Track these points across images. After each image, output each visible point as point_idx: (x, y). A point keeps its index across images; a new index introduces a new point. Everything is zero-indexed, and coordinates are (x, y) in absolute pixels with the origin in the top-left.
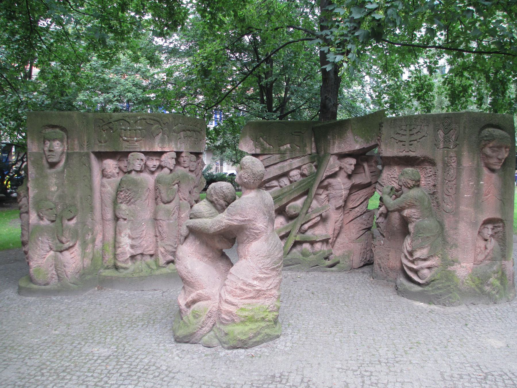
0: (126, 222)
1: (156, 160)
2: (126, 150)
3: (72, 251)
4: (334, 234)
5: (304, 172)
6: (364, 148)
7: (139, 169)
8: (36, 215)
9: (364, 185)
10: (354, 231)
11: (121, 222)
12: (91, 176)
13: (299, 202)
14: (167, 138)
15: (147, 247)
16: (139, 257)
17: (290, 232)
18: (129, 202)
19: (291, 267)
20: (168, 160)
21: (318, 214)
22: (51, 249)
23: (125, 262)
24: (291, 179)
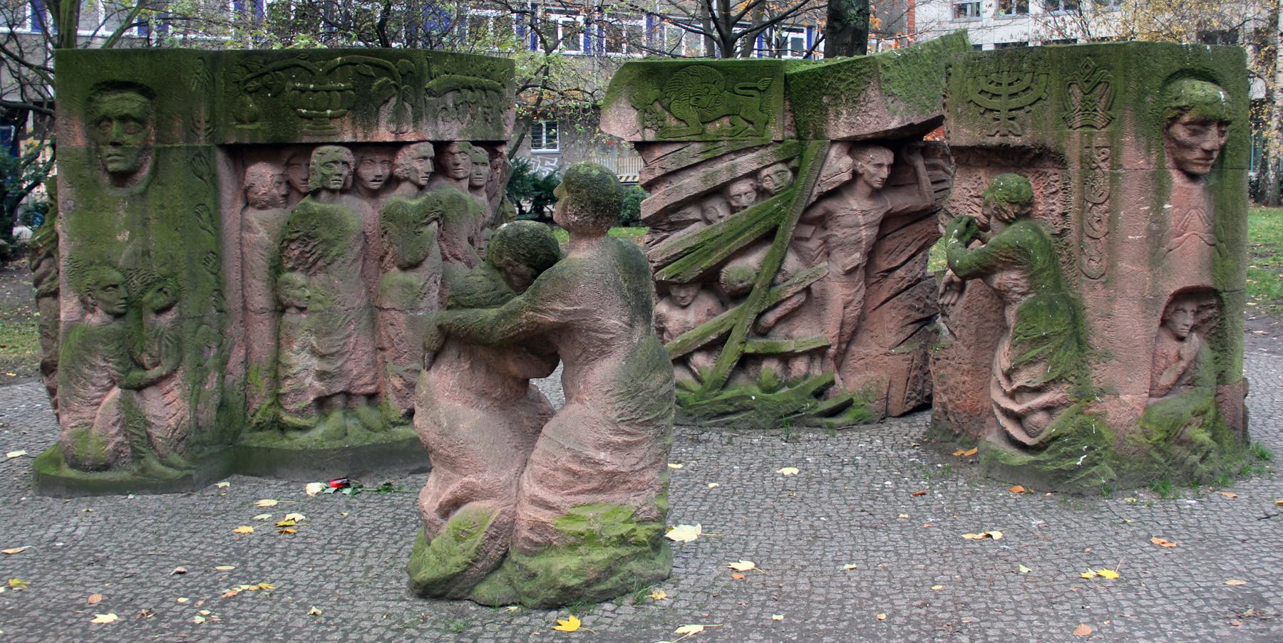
0: (304, 316)
1: (382, 162)
2: (306, 140)
3: (168, 388)
4: (840, 335)
5: (765, 185)
6: (911, 125)
7: (339, 186)
8: (76, 300)
9: (918, 213)
10: (891, 325)
11: (291, 317)
12: (217, 204)
13: (753, 261)
14: (410, 109)
15: (360, 376)
16: (339, 401)
17: (729, 333)
18: (309, 268)
19: (733, 418)
20: (414, 162)
21: (801, 287)
22: (114, 383)
23: (301, 413)
24: (734, 204)
